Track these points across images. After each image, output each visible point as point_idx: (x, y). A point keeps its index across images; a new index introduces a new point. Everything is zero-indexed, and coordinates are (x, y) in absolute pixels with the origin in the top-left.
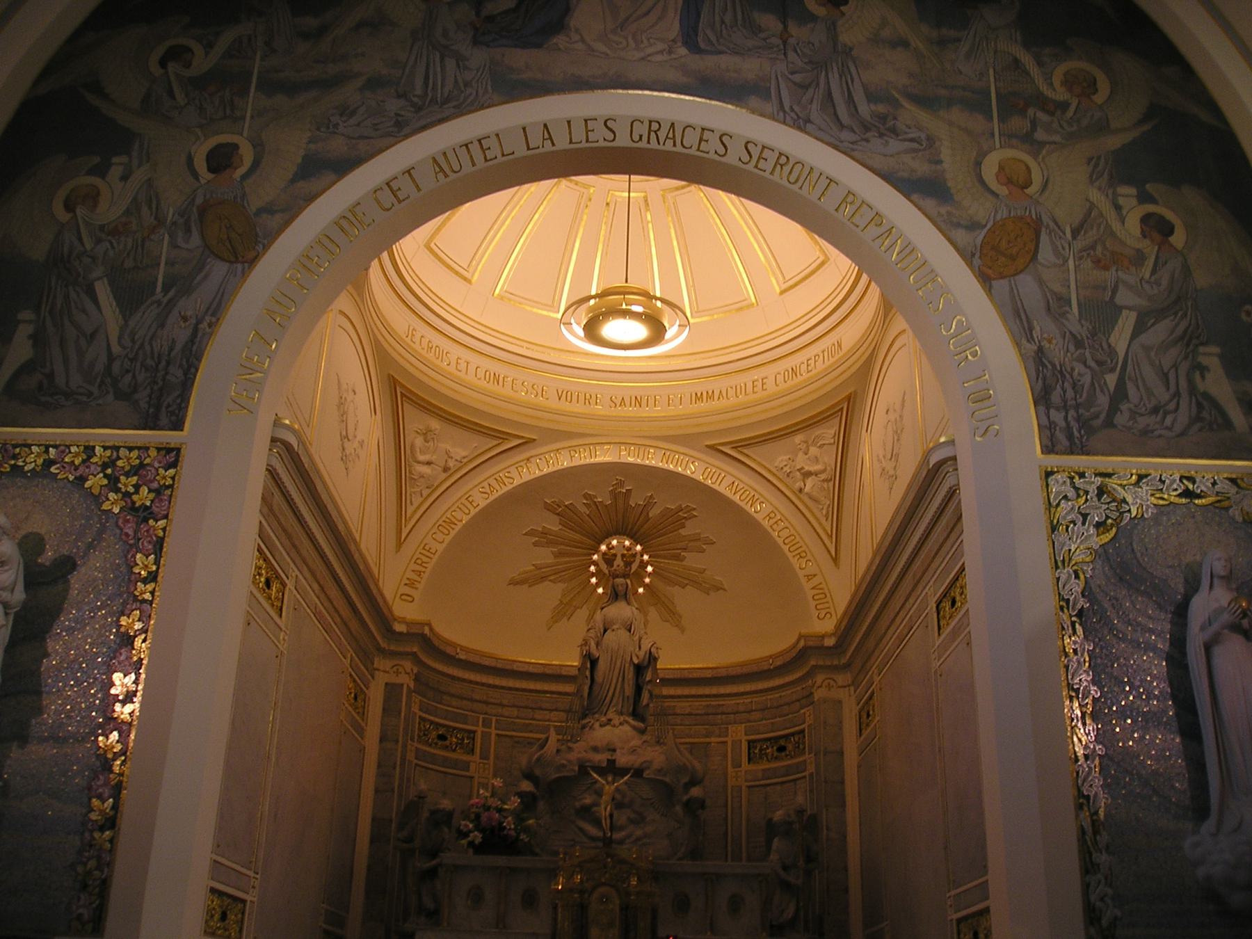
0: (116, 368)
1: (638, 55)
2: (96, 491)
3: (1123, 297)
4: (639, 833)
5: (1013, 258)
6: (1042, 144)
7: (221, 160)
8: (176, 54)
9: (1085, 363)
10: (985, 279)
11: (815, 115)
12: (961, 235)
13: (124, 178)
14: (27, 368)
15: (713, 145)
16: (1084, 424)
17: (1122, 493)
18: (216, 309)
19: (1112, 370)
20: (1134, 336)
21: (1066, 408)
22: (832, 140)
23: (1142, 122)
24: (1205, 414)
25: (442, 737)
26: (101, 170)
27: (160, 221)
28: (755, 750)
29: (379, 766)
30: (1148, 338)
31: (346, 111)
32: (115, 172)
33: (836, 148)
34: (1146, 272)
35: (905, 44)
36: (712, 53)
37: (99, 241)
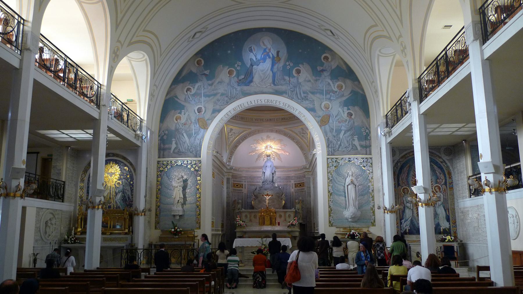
0: (189, 147)
1: (265, 86)
2: (190, 168)
3: (343, 128)
4: (273, 204)
5: (325, 122)
6: (332, 100)
7: (199, 110)
8: (188, 90)
9: (335, 140)
10: (320, 126)
11: (294, 97)
12: (317, 118)
13: (184, 114)
14: (175, 148)
15: (278, 103)
16: (334, 150)
17: (339, 161)
18: (203, 137)
19: (339, 141)
20: (344, 135)
21: (331, 148)
22: (297, 102)
23: (350, 94)
24: (353, 148)
25: (237, 186)
26: (180, 113)
27: (192, 122)
28: (296, 186)
29: (227, 193)
30: (346, 135)
31: (218, 100)
32: (183, 113)
33: (297, 103)
34: (347, 123)
35: (310, 81)
36: (277, 85)
37: (183, 126)
